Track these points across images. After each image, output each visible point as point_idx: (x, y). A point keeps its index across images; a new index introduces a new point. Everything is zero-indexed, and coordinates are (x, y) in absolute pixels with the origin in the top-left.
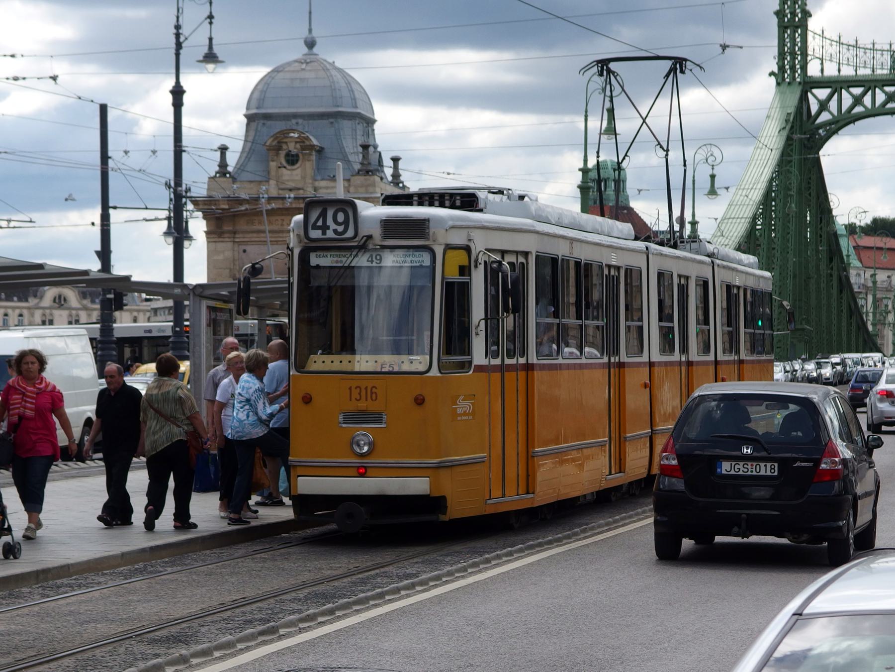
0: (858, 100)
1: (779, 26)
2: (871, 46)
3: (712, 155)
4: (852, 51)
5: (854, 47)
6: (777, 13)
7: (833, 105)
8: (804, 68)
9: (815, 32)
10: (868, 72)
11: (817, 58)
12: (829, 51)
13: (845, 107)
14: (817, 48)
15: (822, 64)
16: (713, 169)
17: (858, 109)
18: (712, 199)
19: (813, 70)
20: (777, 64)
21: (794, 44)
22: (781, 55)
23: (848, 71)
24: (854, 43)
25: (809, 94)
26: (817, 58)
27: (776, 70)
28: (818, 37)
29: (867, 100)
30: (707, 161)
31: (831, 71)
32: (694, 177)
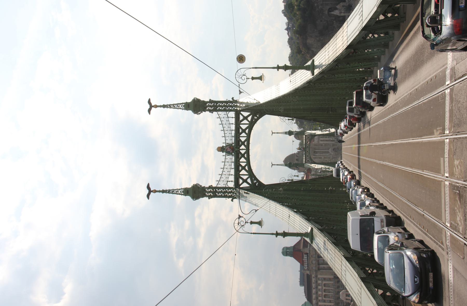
0: (244, 168)
1: (214, 197)
2: (224, 163)
5: (223, 169)
6: (209, 199)
7: (245, 177)
8: (230, 188)
9: (217, 184)
10: (233, 164)
11: (227, 183)
12: (225, 178)
13: (247, 173)
15: (229, 181)
17: (247, 168)
18: (264, 223)
20: (228, 198)
21: (221, 192)
23: (233, 172)
24: (222, 170)
25: (241, 186)
26: (227, 183)
27: (232, 198)
28: (219, 183)
29: (243, 164)
31: (232, 178)
32: (251, 233)
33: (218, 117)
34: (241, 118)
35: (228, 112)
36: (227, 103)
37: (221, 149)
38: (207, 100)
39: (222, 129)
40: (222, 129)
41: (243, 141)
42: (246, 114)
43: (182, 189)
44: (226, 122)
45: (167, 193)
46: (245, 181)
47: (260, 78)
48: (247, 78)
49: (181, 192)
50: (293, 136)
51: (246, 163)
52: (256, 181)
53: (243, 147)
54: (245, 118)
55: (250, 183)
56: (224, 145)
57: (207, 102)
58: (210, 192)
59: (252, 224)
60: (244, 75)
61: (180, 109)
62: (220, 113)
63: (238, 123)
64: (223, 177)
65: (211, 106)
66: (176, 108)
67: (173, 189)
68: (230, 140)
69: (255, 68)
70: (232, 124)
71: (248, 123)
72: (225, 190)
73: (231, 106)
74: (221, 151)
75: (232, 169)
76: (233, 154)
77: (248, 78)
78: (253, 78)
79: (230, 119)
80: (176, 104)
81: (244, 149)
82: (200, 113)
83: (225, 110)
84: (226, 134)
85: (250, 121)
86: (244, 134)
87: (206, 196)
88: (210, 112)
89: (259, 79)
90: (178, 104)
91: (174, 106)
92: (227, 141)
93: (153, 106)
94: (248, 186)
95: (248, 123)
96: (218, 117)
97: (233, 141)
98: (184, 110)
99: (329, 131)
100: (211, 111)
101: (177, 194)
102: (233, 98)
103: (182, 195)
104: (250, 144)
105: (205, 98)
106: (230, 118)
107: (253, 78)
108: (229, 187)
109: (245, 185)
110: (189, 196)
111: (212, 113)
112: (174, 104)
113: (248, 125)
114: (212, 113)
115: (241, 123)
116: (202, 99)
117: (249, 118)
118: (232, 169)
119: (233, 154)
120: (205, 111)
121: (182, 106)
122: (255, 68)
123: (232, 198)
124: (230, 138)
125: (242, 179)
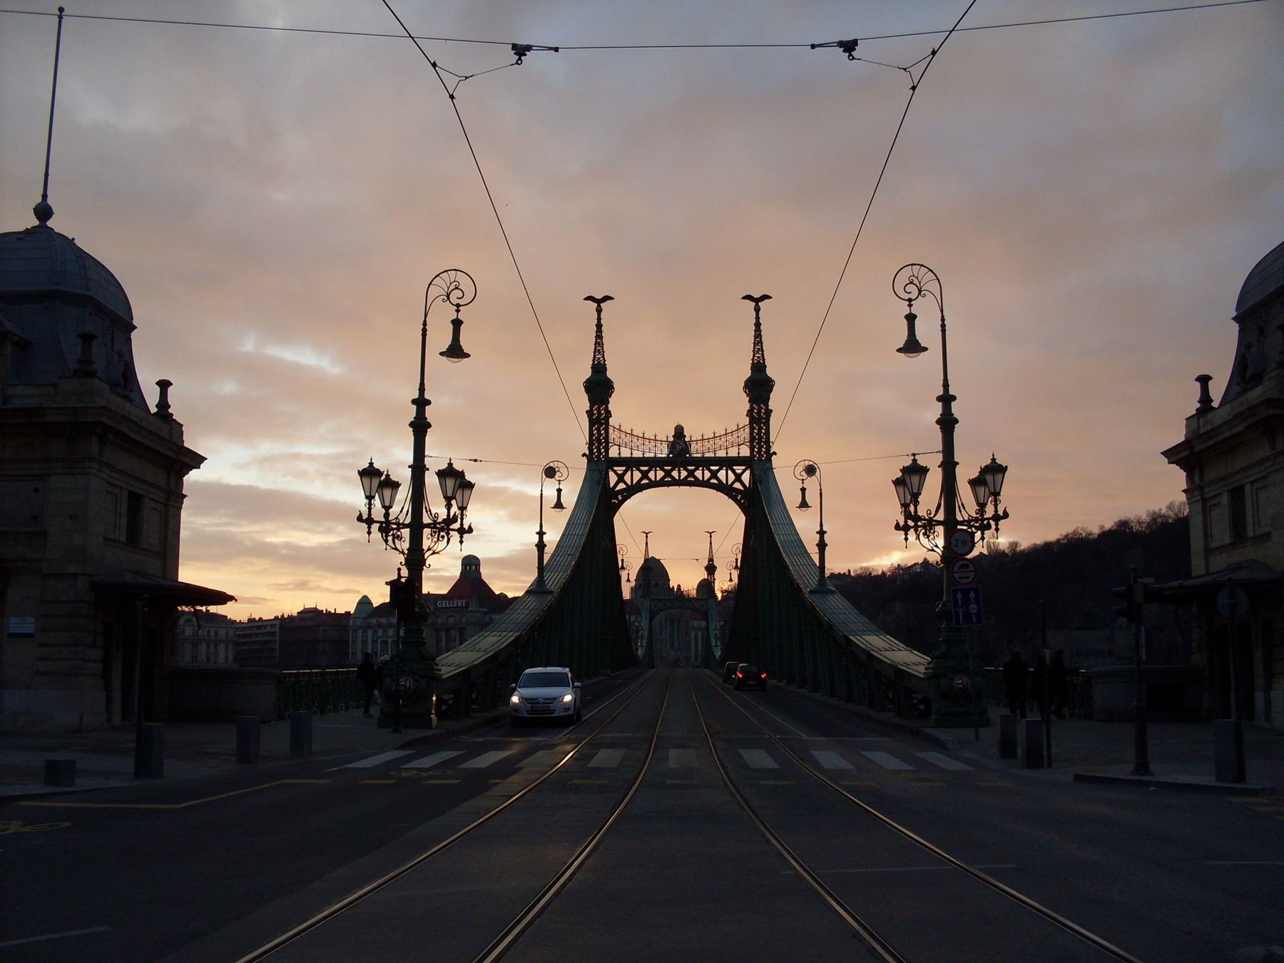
0: (645, 475)
1: (589, 421)
3: (457, 288)
4: (641, 441)
6: (587, 412)
7: (627, 478)
10: (652, 455)
12: (625, 440)
14: (615, 437)
15: (619, 449)
16: (458, 311)
17: (645, 481)
19: (613, 452)
21: (600, 435)
22: (591, 443)
23: (637, 454)
27: (587, 453)
29: (651, 475)
30: (448, 298)
31: (626, 453)
32: (425, 324)
33: (739, 427)
34: (739, 469)
35: (748, 444)
36: (765, 443)
37: (679, 432)
38: (772, 404)
39: (716, 435)
40: (716, 435)
41: (696, 474)
42: (746, 477)
43: (605, 361)
44: (731, 441)
45: (597, 333)
46: (621, 478)
47: (912, 346)
48: (910, 300)
49: (599, 358)
50: (704, 575)
51: (653, 480)
52: (620, 498)
53: (684, 473)
54: (738, 478)
55: (617, 489)
56: (687, 439)
57: (767, 406)
58: (599, 412)
59: (451, 326)
60: (920, 291)
61: (754, 356)
62: (747, 430)
63: (728, 463)
64: (628, 438)
65: (759, 412)
66: (754, 348)
67: (604, 352)
68: (696, 451)
69: (943, 326)
70: (727, 453)
71: (729, 483)
72: (603, 441)
73: (760, 450)
74: (675, 433)
75: (643, 454)
76: (671, 456)
77: (912, 303)
78: (911, 318)
79: (736, 449)
80: (762, 346)
81: (679, 476)
82: (746, 393)
83: (752, 439)
84: (708, 442)
85: (734, 486)
86: (708, 475)
87: (591, 407)
88: (748, 411)
89: (909, 336)
90: (763, 351)
91: (758, 344)
92: (695, 445)
93: (757, 304)
94: (611, 486)
95: (729, 483)
96: (739, 427)
97: (695, 455)
98: (751, 362)
99: (716, 646)
100: (750, 413)
101: (595, 352)
102: (775, 453)
103: (594, 361)
104: (689, 487)
105: (776, 401)
106: (739, 449)
107: (911, 318)
108: (609, 449)
109: (613, 479)
110: (590, 374)
111: (747, 415)
112: (762, 344)
113: (725, 482)
114: (747, 415)
115: (729, 471)
116: (773, 396)
117: (737, 485)
118: (643, 454)
119: (671, 456)
120: (749, 402)
121: (759, 357)
122: (943, 326)
123: (587, 453)
124: (700, 449)
125: (625, 472)
